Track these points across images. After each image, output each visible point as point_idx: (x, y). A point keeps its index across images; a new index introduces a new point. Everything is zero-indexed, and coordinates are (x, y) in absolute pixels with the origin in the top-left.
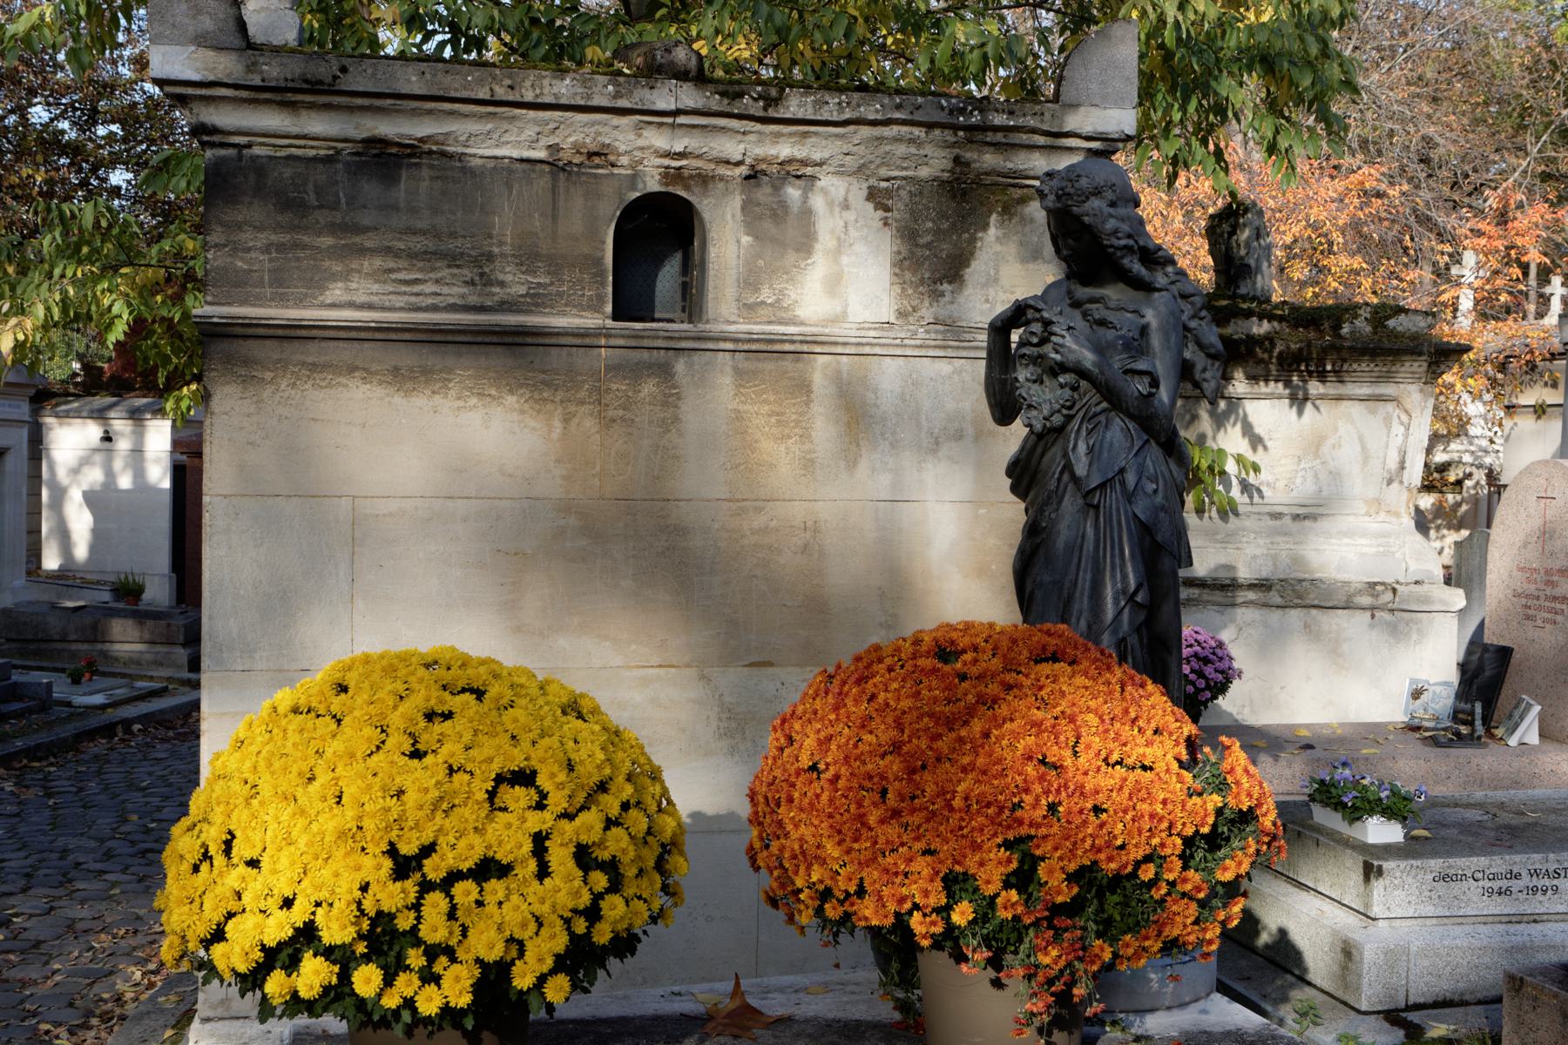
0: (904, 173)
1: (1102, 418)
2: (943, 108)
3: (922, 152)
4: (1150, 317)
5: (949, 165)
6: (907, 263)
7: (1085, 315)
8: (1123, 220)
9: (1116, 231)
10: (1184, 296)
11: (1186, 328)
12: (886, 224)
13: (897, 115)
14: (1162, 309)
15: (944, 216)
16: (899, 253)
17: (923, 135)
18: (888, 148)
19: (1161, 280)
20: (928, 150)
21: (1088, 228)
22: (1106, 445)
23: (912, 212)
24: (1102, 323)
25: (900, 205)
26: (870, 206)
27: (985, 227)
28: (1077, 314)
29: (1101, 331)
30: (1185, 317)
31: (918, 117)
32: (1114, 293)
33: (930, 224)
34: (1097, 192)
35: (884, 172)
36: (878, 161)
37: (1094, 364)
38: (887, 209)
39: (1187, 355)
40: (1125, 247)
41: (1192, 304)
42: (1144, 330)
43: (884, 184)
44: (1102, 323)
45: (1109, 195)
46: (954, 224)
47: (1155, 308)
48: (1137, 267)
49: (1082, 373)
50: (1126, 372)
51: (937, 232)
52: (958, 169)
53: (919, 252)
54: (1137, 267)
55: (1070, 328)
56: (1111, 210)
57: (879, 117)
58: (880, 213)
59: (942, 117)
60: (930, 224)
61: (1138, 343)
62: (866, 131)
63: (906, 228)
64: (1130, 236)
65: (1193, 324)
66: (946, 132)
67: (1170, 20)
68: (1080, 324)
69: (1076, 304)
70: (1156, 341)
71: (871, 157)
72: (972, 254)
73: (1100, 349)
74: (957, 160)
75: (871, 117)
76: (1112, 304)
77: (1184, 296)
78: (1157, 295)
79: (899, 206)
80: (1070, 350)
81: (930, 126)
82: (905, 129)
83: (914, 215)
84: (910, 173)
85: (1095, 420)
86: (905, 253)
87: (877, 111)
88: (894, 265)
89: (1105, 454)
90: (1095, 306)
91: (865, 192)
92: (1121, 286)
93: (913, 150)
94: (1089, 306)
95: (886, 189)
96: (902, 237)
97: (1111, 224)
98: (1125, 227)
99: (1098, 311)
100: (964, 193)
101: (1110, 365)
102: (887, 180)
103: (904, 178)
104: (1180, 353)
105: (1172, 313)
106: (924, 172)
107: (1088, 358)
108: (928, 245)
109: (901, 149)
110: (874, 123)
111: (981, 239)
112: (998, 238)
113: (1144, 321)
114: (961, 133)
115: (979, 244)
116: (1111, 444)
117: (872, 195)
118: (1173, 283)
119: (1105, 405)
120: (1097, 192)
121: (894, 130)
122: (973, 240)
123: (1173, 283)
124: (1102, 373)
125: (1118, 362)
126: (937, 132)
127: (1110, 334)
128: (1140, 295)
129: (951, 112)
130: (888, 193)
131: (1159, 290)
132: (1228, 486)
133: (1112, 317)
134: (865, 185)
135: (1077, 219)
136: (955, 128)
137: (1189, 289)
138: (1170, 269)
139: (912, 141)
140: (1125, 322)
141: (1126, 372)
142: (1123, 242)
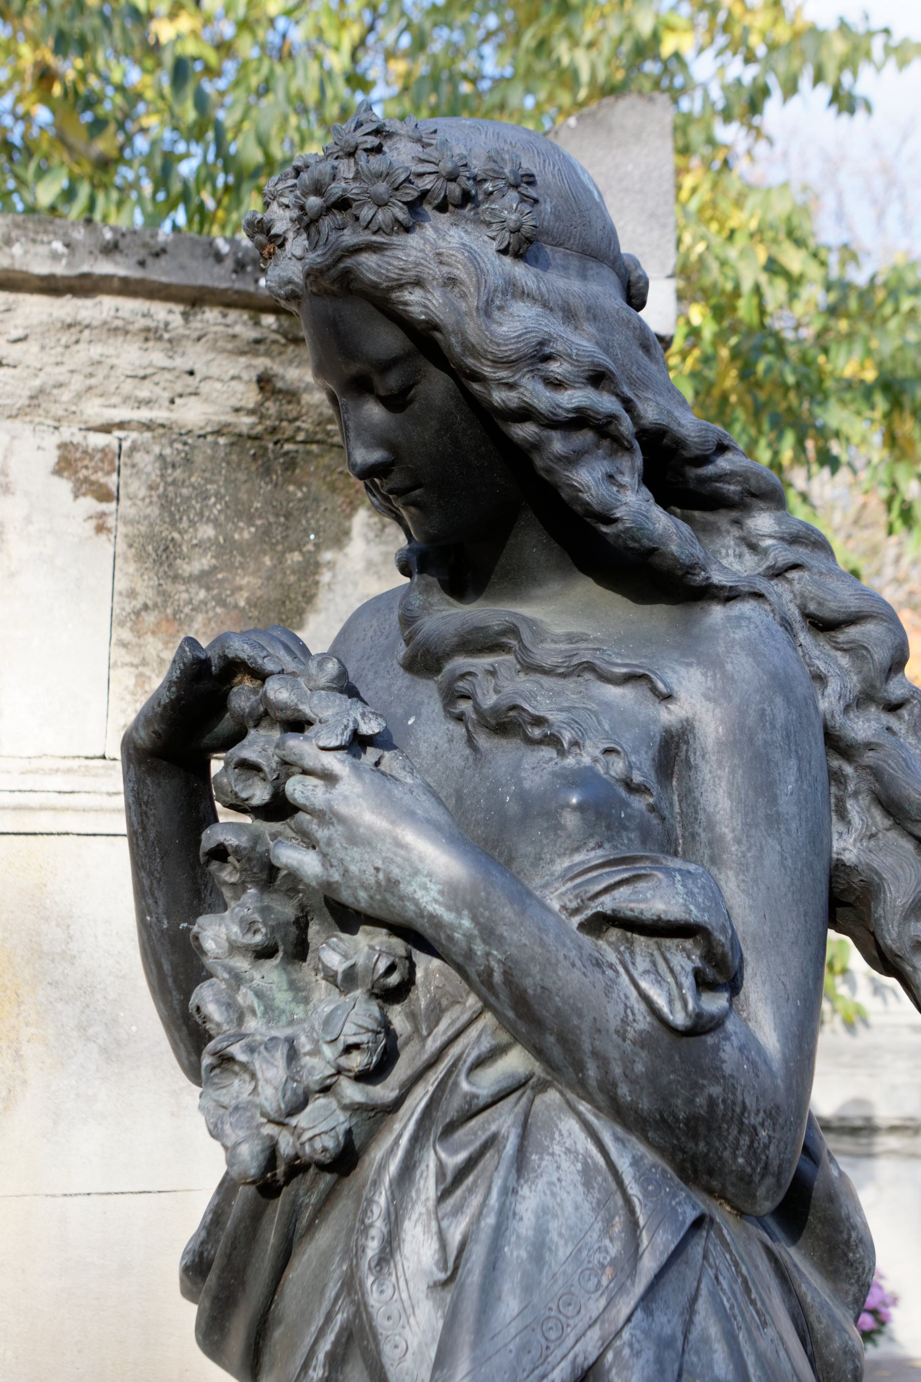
0: (144, 414)
1: (504, 1121)
2: (219, 258)
3: (182, 363)
4: (696, 700)
5: (252, 397)
6: (150, 619)
7: (451, 696)
8: (569, 315)
9: (539, 355)
10: (823, 625)
11: (835, 743)
12: (100, 529)
13: (105, 267)
14: (741, 666)
15: (246, 514)
16: (132, 594)
17: (176, 320)
18: (96, 351)
19: (730, 563)
20: (194, 356)
21: (425, 339)
22: (516, 1253)
23: (166, 503)
24: (507, 723)
25: (136, 487)
26: (64, 486)
27: (340, 538)
28: (428, 693)
29: (503, 753)
30: (828, 702)
31: (159, 273)
32: (564, 613)
33: (207, 531)
34: (460, 197)
35: (96, 410)
36: (77, 383)
37: (454, 895)
38: (104, 495)
39: (847, 846)
40: (580, 420)
41: (854, 650)
42: (672, 752)
43: (98, 440)
44: (507, 723)
45: (508, 208)
46: (266, 532)
47: (712, 664)
48: (633, 505)
49: (415, 936)
50: (599, 924)
51: (225, 549)
52: (272, 407)
53: (181, 593)
54: (633, 505)
55: (358, 743)
56: (520, 271)
57: (60, 269)
58: (89, 504)
59: (219, 278)
60: (207, 531)
61: (647, 808)
62: (35, 308)
63: (150, 537)
64: (598, 378)
65: (863, 727)
66: (233, 315)
67: (747, 286)
68: (432, 731)
69: (424, 661)
70: (719, 791)
71: (60, 374)
72: (309, 598)
73: (491, 836)
74: (264, 382)
75: (41, 268)
76: (548, 653)
77: (823, 625)
78: (717, 613)
79: (136, 488)
80: (355, 837)
81: (194, 299)
82: (130, 306)
83: (171, 507)
84: (159, 414)
85: (474, 1132)
86: (146, 594)
87: (55, 257)
88: (115, 621)
89: (510, 1305)
90: (485, 661)
91: (52, 456)
92: (586, 589)
93: (158, 357)
94: (461, 663)
95: (103, 451)
96: (140, 558)
97: (517, 323)
98: (580, 343)
99: (495, 682)
100: (291, 463)
101: (524, 897)
102: (106, 429)
103: (148, 426)
104: (818, 838)
105: (780, 683)
106: (193, 414)
107: (430, 867)
108: (203, 579)
109: (130, 355)
110: (51, 287)
111: (331, 565)
112: (370, 565)
113: (669, 716)
114: (269, 320)
115: (325, 577)
116: (540, 1250)
117: (68, 462)
118: (778, 573)
119: (516, 1062)
120: (460, 197)
121: (105, 307)
122: (311, 568)
123: (778, 573)
124: (488, 933)
125: (563, 877)
126: (211, 315)
127: (536, 767)
128: (655, 617)
129: (240, 267)
130: (113, 460)
131: (729, 596)
132: (853, 987)
133: (543, 699)
134: (51, 441)
135: (382, 303)
136: (255, 306)
137: (839, 599)
138: (763, 522)
139: (150, 334)
140: (602, 726)
141: (599, 924)
142: (574, 398)
